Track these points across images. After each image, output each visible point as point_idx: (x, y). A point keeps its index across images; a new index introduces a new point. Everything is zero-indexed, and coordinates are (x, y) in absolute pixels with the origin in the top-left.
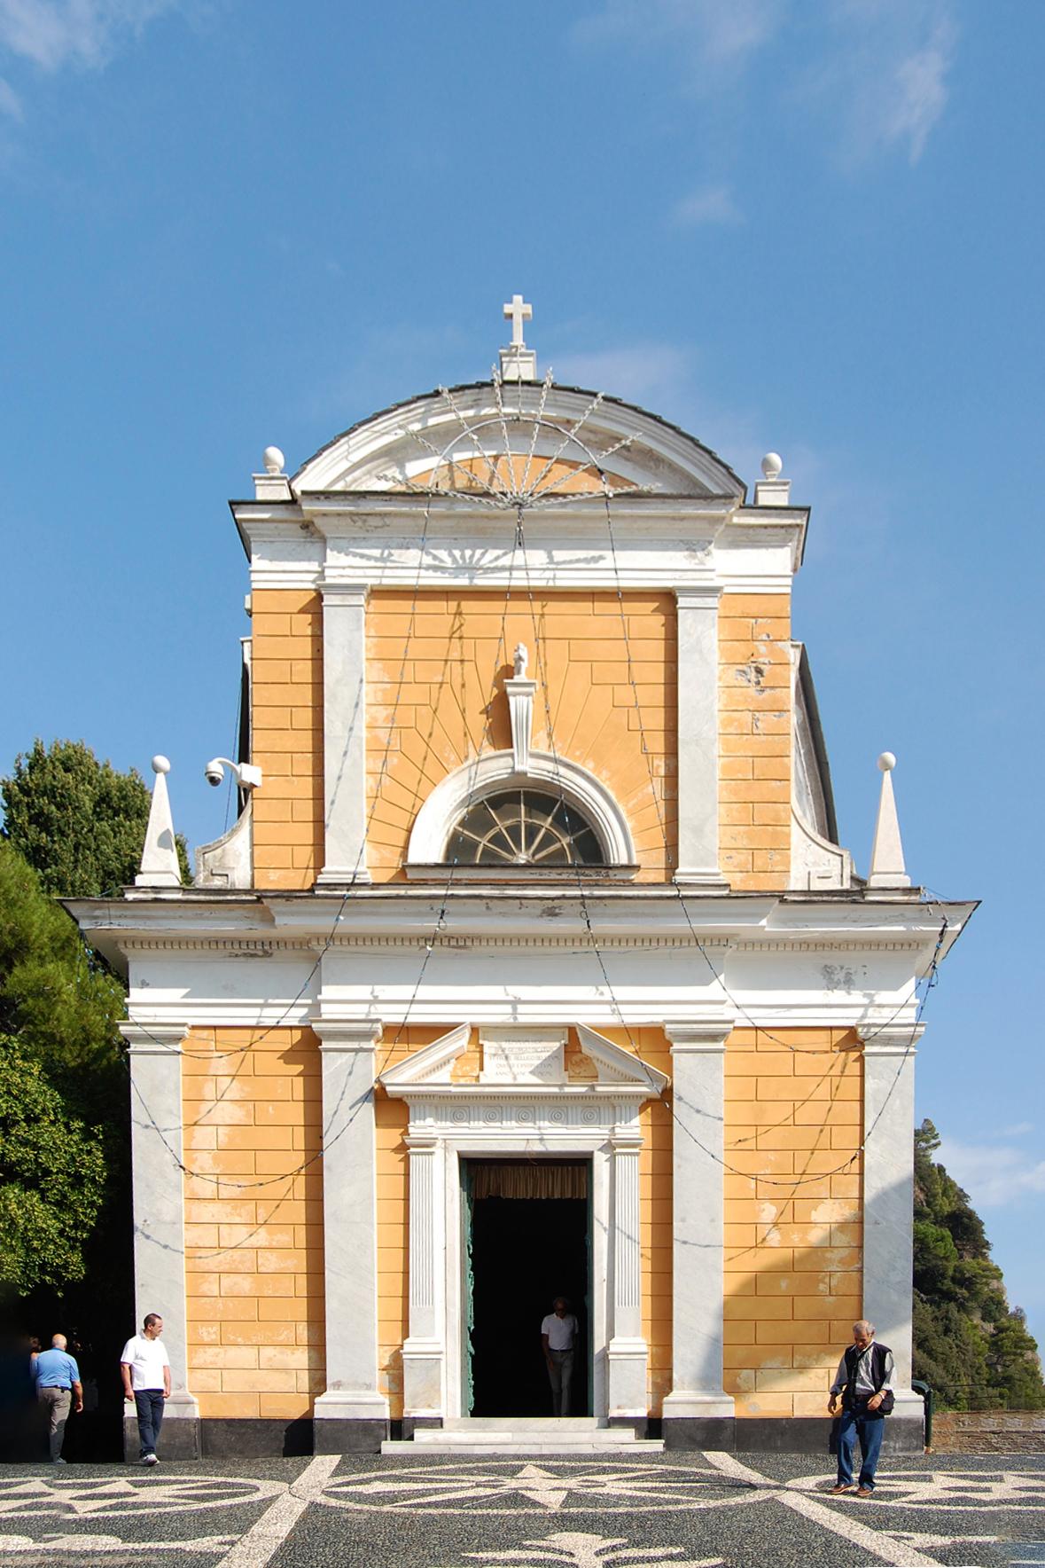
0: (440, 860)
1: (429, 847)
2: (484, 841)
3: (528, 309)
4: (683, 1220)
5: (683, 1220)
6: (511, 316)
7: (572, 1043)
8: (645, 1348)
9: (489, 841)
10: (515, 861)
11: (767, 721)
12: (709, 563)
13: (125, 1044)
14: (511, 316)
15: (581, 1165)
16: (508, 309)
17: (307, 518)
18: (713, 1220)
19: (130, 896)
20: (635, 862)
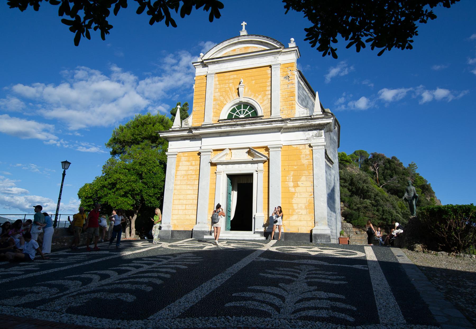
0: (226, 118)
1: (224, 115)
2: (235, 114)
3: (246, 23)
4: (271, 187)
5: (271, 187)
6: (242, 25)
7: (250, 152)
8: (263, 215)
9: (236, 114)
10: (240, 117)
11: (290, 86)
12: (278, 59)
13: (167, 156)
14: (242, 25)
15: (250, 176)
16: (242, 24)
17: (205, 63)
18: (278, 186)
19: (170, 130)
20: (263, 115)
